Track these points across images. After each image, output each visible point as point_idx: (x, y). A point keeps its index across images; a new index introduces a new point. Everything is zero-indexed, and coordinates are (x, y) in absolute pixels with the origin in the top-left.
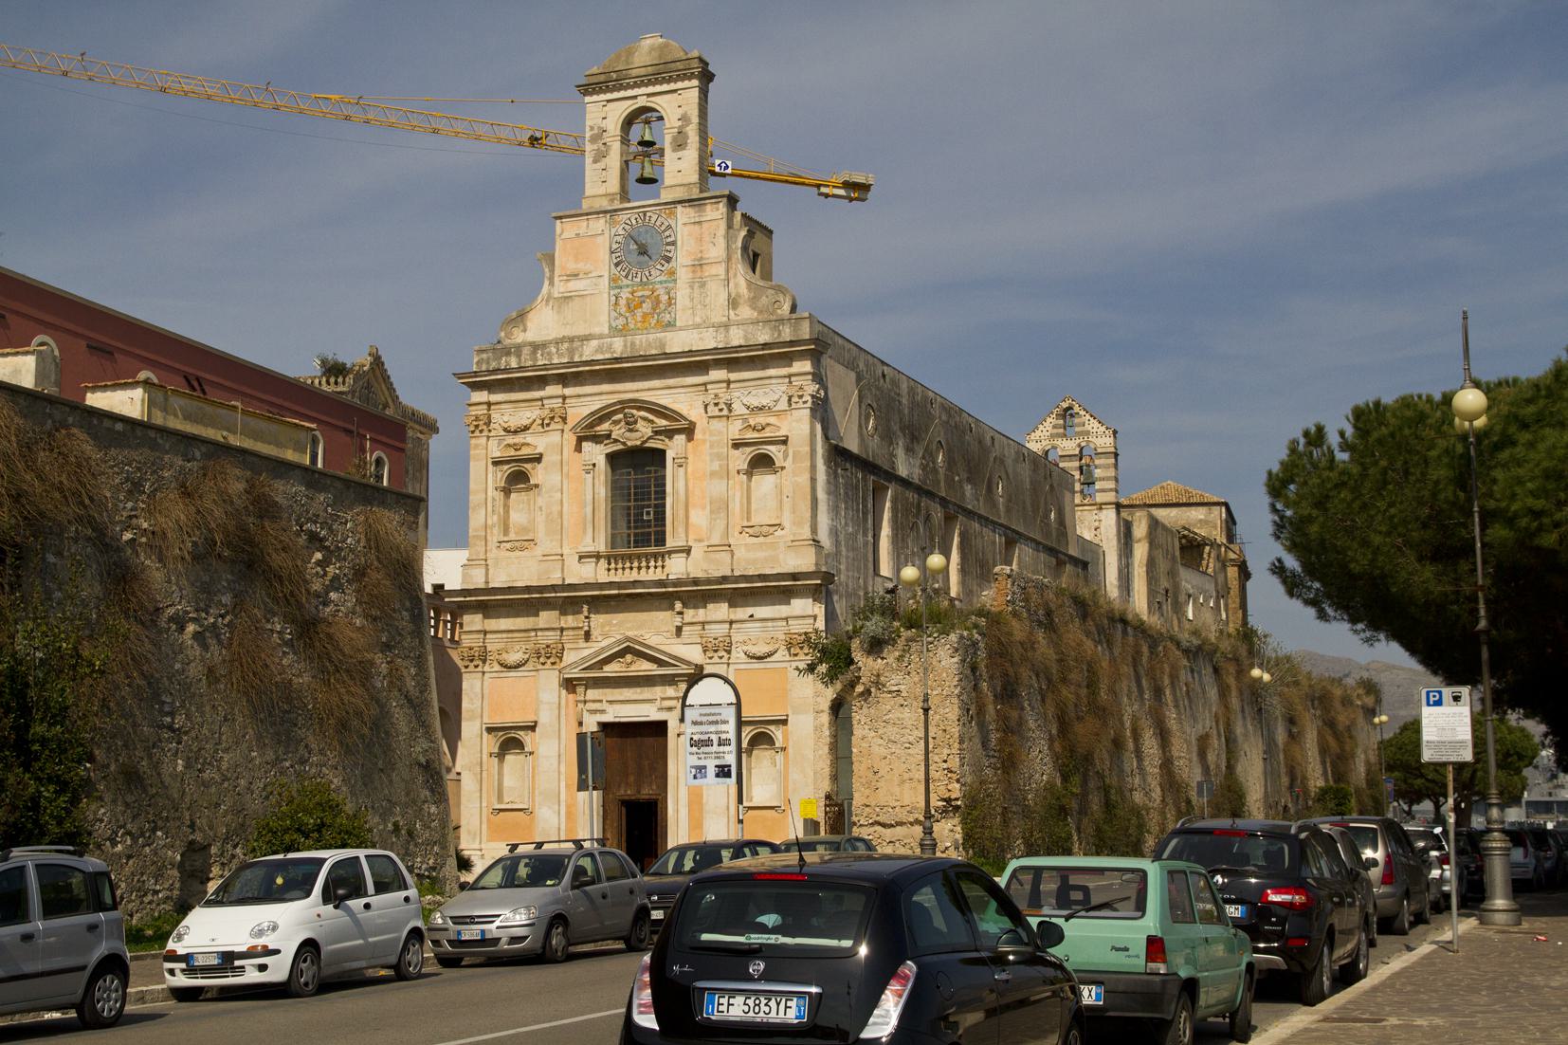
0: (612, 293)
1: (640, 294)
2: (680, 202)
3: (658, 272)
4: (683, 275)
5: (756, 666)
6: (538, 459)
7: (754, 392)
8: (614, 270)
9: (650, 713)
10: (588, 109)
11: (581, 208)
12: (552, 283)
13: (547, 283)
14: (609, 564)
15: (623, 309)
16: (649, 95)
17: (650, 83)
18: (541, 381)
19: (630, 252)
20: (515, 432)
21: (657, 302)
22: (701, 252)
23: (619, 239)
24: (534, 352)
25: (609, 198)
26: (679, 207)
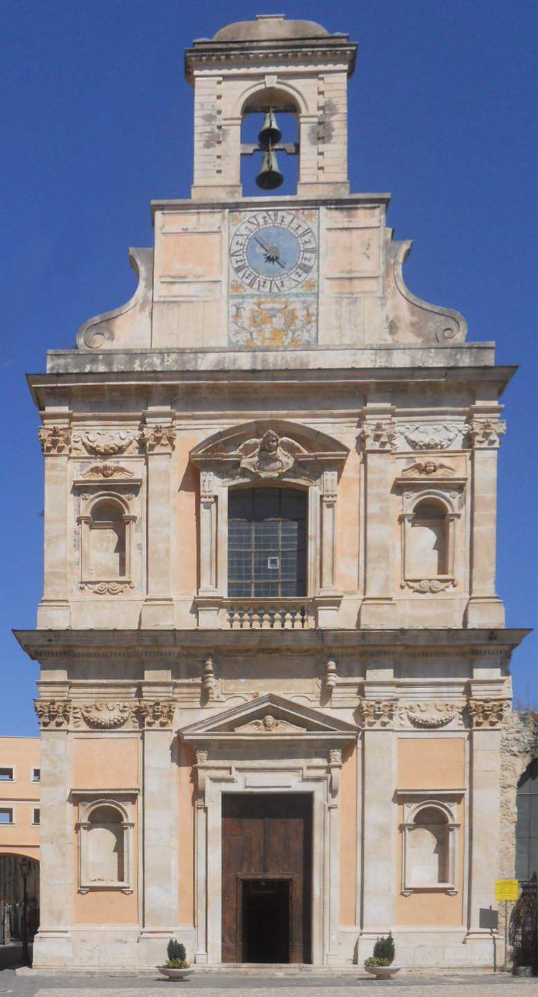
0: (231, 302)
1: (269, 306)
2: (325, 202)
3: (294, 284)
4: (327, 290)
5: (426, 735)
6: (133, 488)
7: (422, 428)
8: (233, 276)
9: (291, 783)
10: (197, 84)
11: (190, 197)
12: (151, 284)
13: (142, 284)
14: (232, 615)
15: (246, 323)
16: (280, 75)
17: (285, 60)
18: (145, 395)
19: (256, 256)
20: (106, 455)
21: (291, 317)
22: (351, 263)
23: (241, 239)
24: (131, 362)
25: (231, 189)
26: (323, 209)
